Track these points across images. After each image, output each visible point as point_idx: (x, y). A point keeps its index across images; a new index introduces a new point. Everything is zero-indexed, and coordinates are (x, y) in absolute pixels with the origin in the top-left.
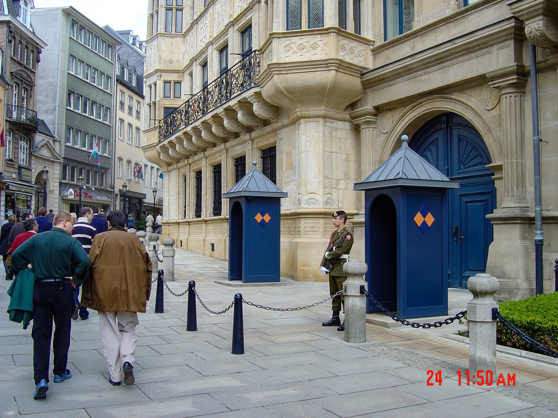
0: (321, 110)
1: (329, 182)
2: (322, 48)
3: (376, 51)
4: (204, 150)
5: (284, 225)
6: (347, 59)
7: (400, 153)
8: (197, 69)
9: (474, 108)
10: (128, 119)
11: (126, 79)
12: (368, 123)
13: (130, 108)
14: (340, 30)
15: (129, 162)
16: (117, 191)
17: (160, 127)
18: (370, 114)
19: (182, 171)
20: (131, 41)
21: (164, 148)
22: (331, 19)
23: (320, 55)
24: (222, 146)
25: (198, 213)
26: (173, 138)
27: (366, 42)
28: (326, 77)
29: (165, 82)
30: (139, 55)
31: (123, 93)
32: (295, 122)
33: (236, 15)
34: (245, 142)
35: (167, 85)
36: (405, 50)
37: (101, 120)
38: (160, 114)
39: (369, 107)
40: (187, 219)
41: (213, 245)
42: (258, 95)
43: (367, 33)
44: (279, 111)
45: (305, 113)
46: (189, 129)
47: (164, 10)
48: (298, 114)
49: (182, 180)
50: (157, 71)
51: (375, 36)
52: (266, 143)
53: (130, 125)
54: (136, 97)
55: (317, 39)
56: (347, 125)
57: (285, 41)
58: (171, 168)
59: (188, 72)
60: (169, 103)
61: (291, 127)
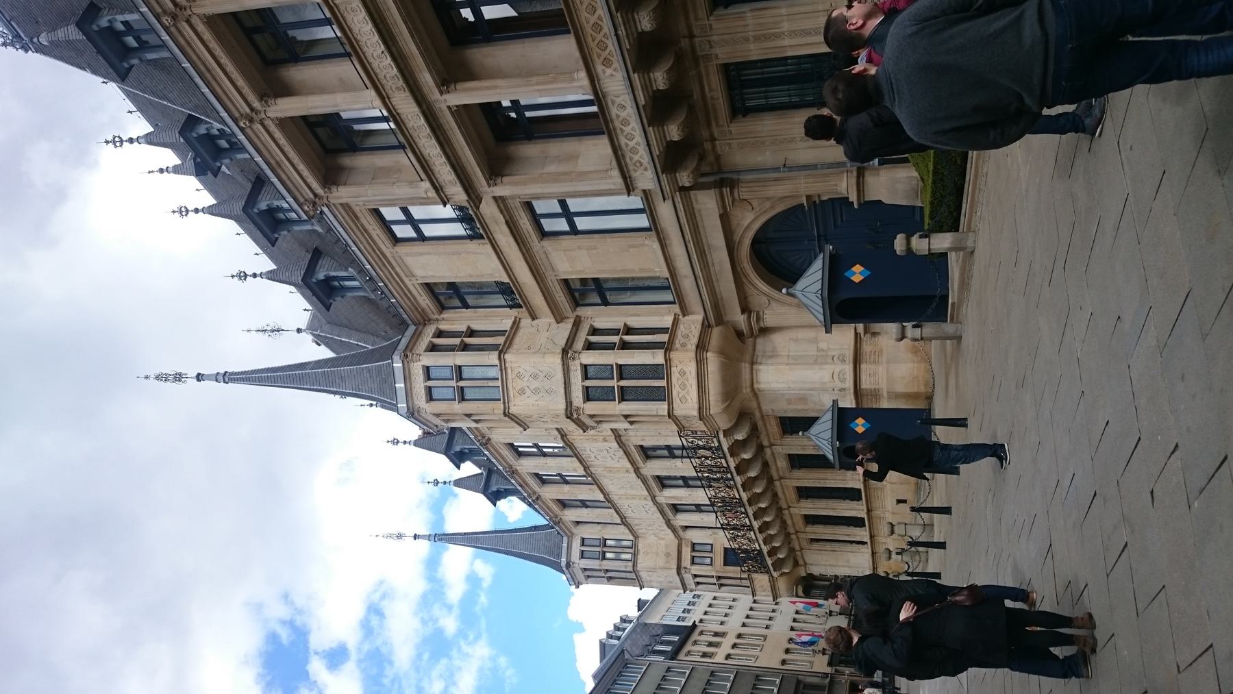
0: (745, 367)
1: (820, 359)
2: (684, 364)
4: (780, 509)
5: (867, 404)
6: (695, 340)
7: (799, 294)
8: (682, 519)
9: (749, 221)
10: (725, 648)
11: (669, 648)
12: (758, 319)
13: (710, 644)
14: (667, 347)
15: (787, 651)
16: (828, 670)
17: (749, 571)
18: (749, 318)
19: (804, 544)
20: (615, 642)
21: (778, 565)
22: (657, 358)
23: (691, 369)
24: (777, 483)
27: (676, 322)
28: (713, 363)
29: (693, 563)
30: (634, 630)
31: (689, 653)
32: (755, 393)
33: (629, 466)
34: (773, 454)
35: (697, 560)
36: (688, 284)
37: (729, 685)
38: (734, 571)
39: (740, 319)
40: (867, 539)
41: (899, 501)
42: (727, 433)
43: (667, 322)
44: (744, 411)
45: (748, 383)
46: (756, 525)
47: (605, 562)
48: (749, 390)
49: (816, 546)
50: (679, 573)
51: (669, 313)
52: (774, 428)
53: (734, 646)
54: (695, 636)
56: (760, 341)
58: (801, 562)
59: (681, 532)
60: (719, 559)
61: (760, 398)
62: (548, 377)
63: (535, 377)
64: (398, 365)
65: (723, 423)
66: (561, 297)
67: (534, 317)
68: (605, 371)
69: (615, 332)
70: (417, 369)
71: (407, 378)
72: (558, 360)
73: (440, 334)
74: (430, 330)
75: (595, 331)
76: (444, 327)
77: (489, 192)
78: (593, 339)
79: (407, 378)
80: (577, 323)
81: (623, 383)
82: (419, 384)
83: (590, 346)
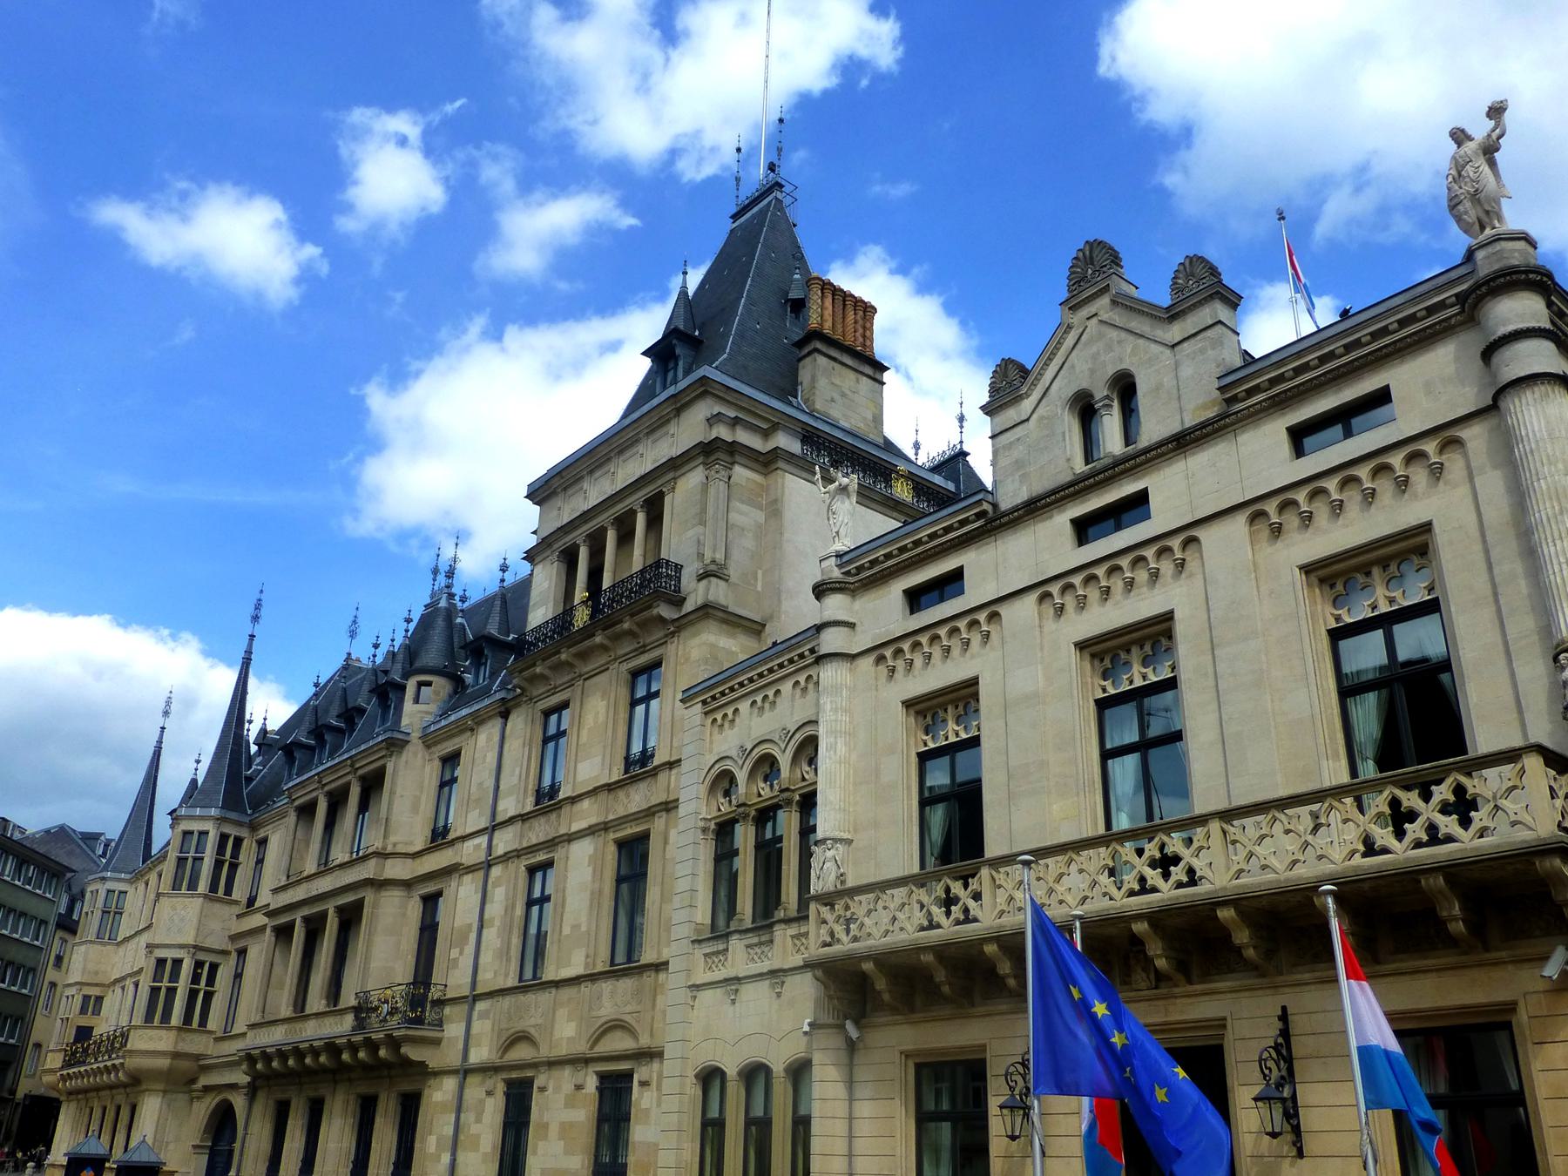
0: (161, 1086)
3: (217, 1040)
16: (20, 1094)
26: (71, 1071)
28: (164, 1063)
38: (70, 1036)
44: (136, 1082)
55: (163, 1033)
57: (140, 1032)
60: (84, 1021)
62: (179, 931)
63: (182, 920)
64: (213, 812)
66: (241, 944)
67: (238, 916)
68: (175, 976)
70: (209, 826)
72: (189, 939)
73: (238, 842)
74: (244, 833)
75: (214, 968)
76: (245, 842)
78: (207, 966)
79: (202, 818)
80: (225, 953)
81: (163, 991)
82: (196, 826)
83: (199, 965)
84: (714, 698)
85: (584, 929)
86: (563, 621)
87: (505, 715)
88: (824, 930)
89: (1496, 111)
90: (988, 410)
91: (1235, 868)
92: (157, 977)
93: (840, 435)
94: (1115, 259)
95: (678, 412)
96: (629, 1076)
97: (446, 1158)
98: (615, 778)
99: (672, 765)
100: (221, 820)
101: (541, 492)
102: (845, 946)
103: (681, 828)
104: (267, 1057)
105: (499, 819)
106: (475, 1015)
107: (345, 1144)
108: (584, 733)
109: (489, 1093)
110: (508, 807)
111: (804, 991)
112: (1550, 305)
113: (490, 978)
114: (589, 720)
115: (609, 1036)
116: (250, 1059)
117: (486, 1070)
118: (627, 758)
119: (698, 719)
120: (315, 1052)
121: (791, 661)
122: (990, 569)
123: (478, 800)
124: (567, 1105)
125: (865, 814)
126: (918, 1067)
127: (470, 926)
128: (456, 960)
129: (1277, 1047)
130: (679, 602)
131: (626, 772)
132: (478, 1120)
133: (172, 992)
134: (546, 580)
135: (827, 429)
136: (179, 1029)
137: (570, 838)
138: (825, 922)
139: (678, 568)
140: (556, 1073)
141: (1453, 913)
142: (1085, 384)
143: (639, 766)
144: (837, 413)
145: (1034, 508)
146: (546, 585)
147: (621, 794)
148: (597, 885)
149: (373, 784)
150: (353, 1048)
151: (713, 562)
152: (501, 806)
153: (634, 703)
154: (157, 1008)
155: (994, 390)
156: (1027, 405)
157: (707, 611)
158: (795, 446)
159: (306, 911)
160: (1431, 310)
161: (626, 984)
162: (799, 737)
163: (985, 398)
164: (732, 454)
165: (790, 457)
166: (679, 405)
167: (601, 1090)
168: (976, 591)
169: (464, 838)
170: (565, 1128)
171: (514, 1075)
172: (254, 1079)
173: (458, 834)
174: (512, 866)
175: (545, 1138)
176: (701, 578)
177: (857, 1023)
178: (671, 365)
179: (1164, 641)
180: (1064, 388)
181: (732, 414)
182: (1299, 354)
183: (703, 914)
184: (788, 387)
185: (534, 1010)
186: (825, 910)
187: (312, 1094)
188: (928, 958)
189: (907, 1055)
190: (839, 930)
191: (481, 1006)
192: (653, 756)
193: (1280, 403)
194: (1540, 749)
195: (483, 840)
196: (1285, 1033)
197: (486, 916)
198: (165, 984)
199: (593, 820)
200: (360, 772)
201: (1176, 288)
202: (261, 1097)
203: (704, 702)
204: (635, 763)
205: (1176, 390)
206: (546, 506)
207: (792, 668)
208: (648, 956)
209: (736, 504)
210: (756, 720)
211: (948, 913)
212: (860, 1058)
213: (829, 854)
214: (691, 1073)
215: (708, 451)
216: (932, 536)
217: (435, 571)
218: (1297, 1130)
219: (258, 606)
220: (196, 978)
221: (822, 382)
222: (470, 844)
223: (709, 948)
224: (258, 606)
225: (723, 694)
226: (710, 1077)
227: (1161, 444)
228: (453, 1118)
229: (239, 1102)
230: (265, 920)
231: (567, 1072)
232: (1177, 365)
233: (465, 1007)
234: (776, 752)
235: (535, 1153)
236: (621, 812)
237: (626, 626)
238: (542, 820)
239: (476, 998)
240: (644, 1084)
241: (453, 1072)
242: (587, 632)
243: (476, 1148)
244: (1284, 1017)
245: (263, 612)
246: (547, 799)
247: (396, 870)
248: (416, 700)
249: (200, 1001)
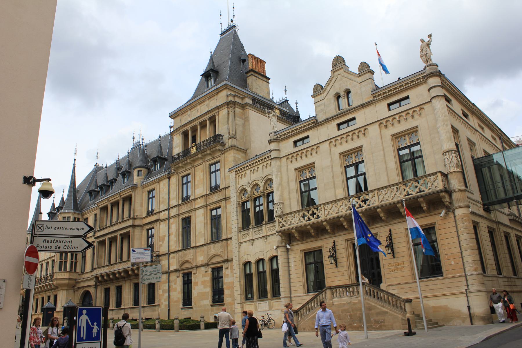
0: (66, 288)
2: (66, 275)
3: (79, 275)
22: (68, 270)
25: (36, 312)
28: (67, 282)
39: (76, 287)
43: (78, 271)
52: (55, 293)
57: (58, 274)
64: (71, 211)
65: (55, 283)
69: (76, 259)
70: (70, 215)
71: (68, 213)
74: (80, 217)
77: (97, 240)
79: (68, 213)
82: (67, 215)
84: (239, 170)
85: (203, 232)
86: (186, 152)
87: (169, 178)
88: (281, 224)
89: (430, 36)
90: (313, 96)
91: (380, 200)
92: (61, 259)
93: (260, 98)
94: (344, 61)
95: (218, 93)
96: (222, 267)
97: (167, 295)
98: (208, 193)
99: (225, 188)
100: (74, 213)
101: (173, 116)
102: (287, 227)
103: (232, 204)
104: (102, 276)
105: (171, 206)
106: (170, 258)
107: (131, 296)
108: (196, 182)
109: (178, 277)
110: (173, 203)
111: (276, 240)
112: (441, 79)
113: (173, 248)
114: (197, 178)
115: (214, 258)
116: (96, 277)
117: (176, 271)
118: (211, 187)
119: (234, 176)
120: (120, 273)
121: (262, 160)
122: (316, 136)
123: (163, 202)
124: (203, 277)
125: (286, 196)
126: (305, 253)
127: (165, 236)
128: (161, 245)
129: (389, 237)
130: (224, 145)
131: (211, 191)
132: (175, 284)
133: (66, 262)
134: (178, 140)
135: (257, 96)
136: (69, 272)
137: (195, 210)
138: (281, 222)
139: (222, 136)
140: (199, 269)
141: (424, 206)
142: (338, 91)
143: (215, 189)
144: (258, 92)
145: (327, 121)
146: (178, 141)
147: (210, 197)
148: (206, 221)
149: (128, 199)
150: (133, 270)
151: (233, 134)
152: (171, 203)
153: (211, 173)
154: (62, 267)
155: (314, 92)
156: (323, 96)
157: (233, 147)
158: (250, 102)
159: (110, 236)
160: (417, 79)
161: (218, 245)
162: (266, 179)
163: (312, 94)
164: (235, 105)
165: (250, 105)
166: (218, 91)
167: (213, 272)
168: (312, 141)
169: (159, 212)
170: (203, 283)
171: (185, 271)
172: (96, 283)
173: (158, 211)
174: (177, 219)
175: (197, 285)
176: (229, 139)
177: (289, 245)
178: (209, 78)
179: (360, 152)
180: (333, 92)
181: (234, 94)
182: (389, 87)
183: (240, 226)
184: (245, 85)
185: (189, 255)
186: (280, 220)
187: (117, 285)
188: (309, 227)
189: (302, 251)
190: (284, 223)
191: (171, 256)
192: (219, 186)
193: (385, 98)
194: (441, 172)
195: (167, 212)
196: (390, 234)
197: (170, 232)
198: (63, 260)
199: (203, 204)
200: (122, 197)
201: (360, 70)
202: (99, 288)
203: (236, 171)
204: (214, 189)
205: (360, 94)
206: (175, 119)
207: (262, 162)
208: (224, 237)
209: (237, 118)
210: (252, 175)
211: (313, 217)
212: (290, 253)
213: (279, 206)
214: (241, 264)
215: (228, 104)
216: (300, 128)
217: (134, 138)
218: (393, 253)
219: (76, 150)
220: (72, 258)
221: (254, 83)
222: (162, 214)
223: (243, 233)
224: (76, 150)
225: (241, 169)
226: (247, 264)
227: (358, 107)
228: (167, 284)
229: (92, 290)
230: (95, 240)
231: (203, 269)
232: (361, 87)
233: (167, 256)
234: (259, 183)
235: (194, 289)
236: (211, 202)
237: (209, 152)
238: (185, 205)
239: (169, 254)
240: (226, 268)
241: (166, 273)
242: (196, 154)
243: (175, 290)
244: (390, 231)
245: (78, 152)
246: (186, 200)
247: (137, 222)
248: (138, 176)
249: (74, 264)
